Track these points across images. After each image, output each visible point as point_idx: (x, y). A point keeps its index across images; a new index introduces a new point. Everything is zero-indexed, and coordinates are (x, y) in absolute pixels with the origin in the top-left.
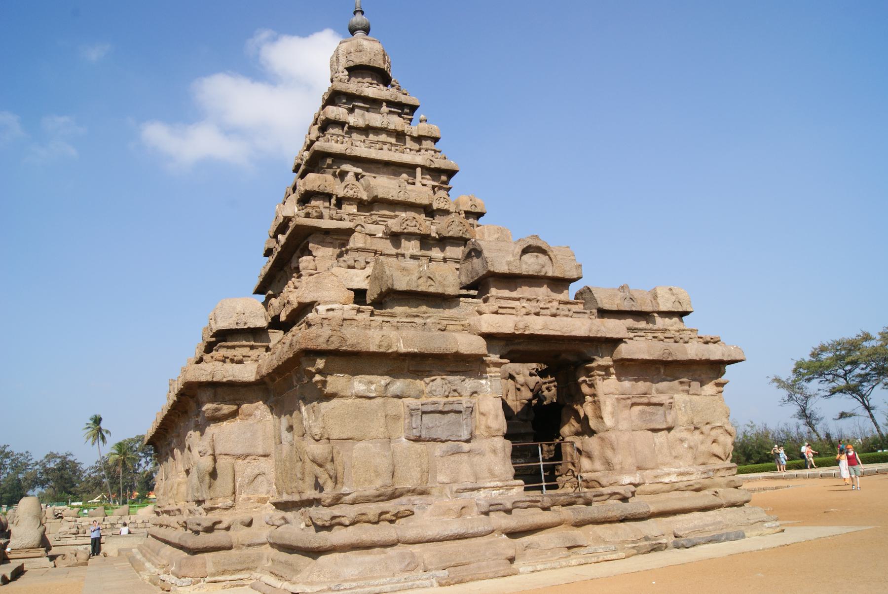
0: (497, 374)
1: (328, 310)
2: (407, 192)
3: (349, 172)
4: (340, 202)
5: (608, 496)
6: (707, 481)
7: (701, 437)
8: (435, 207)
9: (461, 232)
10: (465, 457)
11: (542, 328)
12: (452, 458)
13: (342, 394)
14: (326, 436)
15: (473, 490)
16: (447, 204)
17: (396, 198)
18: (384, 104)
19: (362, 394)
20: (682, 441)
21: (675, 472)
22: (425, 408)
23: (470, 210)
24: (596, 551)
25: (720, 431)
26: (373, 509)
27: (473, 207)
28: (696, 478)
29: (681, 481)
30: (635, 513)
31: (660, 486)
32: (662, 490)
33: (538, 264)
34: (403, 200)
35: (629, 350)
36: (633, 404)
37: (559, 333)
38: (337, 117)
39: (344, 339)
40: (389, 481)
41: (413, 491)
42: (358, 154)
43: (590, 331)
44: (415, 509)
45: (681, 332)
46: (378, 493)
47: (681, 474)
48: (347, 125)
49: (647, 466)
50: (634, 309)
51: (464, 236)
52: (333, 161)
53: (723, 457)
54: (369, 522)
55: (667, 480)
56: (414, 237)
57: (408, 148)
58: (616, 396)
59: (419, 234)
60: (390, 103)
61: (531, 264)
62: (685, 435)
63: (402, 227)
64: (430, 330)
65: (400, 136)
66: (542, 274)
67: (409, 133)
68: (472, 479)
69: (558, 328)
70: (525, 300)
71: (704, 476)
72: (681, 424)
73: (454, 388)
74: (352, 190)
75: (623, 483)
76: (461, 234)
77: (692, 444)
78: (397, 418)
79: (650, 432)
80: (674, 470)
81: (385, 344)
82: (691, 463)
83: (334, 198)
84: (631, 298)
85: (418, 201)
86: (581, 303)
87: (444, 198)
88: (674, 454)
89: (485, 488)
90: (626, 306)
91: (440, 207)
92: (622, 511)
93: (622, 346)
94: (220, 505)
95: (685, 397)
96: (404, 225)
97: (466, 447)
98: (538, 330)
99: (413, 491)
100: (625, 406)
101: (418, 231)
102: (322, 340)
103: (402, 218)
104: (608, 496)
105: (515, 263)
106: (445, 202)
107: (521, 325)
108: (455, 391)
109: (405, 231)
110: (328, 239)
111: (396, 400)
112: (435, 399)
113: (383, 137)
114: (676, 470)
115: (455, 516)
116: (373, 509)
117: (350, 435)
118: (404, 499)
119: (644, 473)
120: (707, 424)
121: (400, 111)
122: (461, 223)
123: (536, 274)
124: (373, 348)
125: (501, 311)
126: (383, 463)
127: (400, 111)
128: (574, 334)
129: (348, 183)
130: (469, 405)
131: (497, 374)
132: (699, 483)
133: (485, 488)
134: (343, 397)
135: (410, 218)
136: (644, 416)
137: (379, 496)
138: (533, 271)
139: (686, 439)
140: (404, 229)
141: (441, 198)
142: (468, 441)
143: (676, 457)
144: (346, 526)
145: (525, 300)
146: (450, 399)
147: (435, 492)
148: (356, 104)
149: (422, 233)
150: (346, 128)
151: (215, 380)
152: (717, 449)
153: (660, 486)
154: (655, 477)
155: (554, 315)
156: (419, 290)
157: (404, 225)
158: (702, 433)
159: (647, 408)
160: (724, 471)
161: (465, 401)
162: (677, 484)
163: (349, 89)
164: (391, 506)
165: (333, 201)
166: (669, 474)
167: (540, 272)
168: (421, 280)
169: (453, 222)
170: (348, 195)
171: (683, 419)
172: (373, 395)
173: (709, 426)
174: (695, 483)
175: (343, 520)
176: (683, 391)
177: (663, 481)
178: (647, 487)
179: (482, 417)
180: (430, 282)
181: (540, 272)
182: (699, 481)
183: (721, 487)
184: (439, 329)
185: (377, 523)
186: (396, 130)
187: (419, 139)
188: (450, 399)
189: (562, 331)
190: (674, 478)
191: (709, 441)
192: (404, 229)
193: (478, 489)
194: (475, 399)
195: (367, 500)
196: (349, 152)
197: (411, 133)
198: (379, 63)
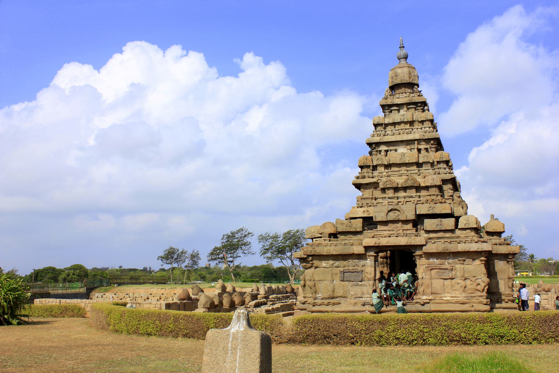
0: (372, 259)
1: (316, 240)
4: (375, 168)
5: (415, 303)
6: (468, 300)
7: (471, 282)
8: (421, 161)
9: (412, 184)
10: (360, 287)
12: (355, 287)
13: (319, 267)
14: (313, 279)
15: (360, 297)
17: (399, 162)
18: (405, 106)
19: (325, 267)
20: (458, 284)
21: (449, 296)
22: (345, 271)
23: (439, 160)
25: (480, 280)
26: (326, 301)
27: (441, 158)
28: (461, 298)
29: (453, 300)
33: (395, 216)
35: (431, 248)
36: (432, 269)
37: (394, 245)
39: (315, 251)
40: (332, 294)
41: (341, 297)
43: (407, 243)
44: (341, 302)
45: (467, 237)
46: (328, 297)
48: (384, 125)
50: (442, 229)
51: (413, 185)
52: (375, 146)
53: (481, 291)
54: (325, 305)
55: (445, 299)
56: (391, 189)
58: (426, 265)
59: (393, 187)
60: (408, 104)
61: (392, 216)
62: (460, 281)
63: (384, 186)
64: (347, 245)
66: (397, 219)
67: (417, 120)
68: (361, 294)
69: (393, 243)
70: (388, 231)
71: (466, 298)
72: (458, 277)
73: (356, 264)
76: (412, 185)
77: (462, 285)
78: (336, 274)
79: (442, 280)
80: (449, 295)
81: (328, 252)
82: (461, 293)
83: (371, 167)
85: (410, 161)
86: (414, 229)
89: (364, 297)
90: (438, 228)
92: (417, 309)
93: (424, 247)
94: (307, 296)
95: (462, 266)
96: (385, 184)
97: (360, 283)
98: (385, 244)
99: (341, 297)
100: (428, 270)
101: (391, 186)
102: (309, 252)
104: (415, 303)
105: (384, 217)
107: (377, 243)
108: (357, 265)
109: (386, 187)
110: (368, 187)
111: (336, 268)
112: (349, 268)
113: (403, 126)
114: (450, 295)
115: (353, 305)
116: (326, 301)
117: (321, 279)
118: (337, 299)
120: (474, 277)
121: (415, 106)
124: (325, 254)
125: (375, 236)
126: (330, 288)
127: (415, 106)
128: (400, 244)
130: (361, 270)
131: (372, 259)
132: (462, 301)
133: (364, 297)
134: (319, 267)
135: (388, 181)
136: (438, 273)
137: (329, 298)
139: (460, 283)
140: (385, 186)
142: (361, 281)
143: (455, 290)
144: (319, 306)
145: (388, 231)
146: (355, 268)
147: (349, 297)
149: (393, 186)
150: (383, 126)
151: (301, 257)
152: (479, 287)
153: (442, 301)
154: (441, 297)
155: (397, 237)
156: (346, 231)
157: (385, 184)
158: (471, 281)
159: (440, 271)
160: (478, 297)
161: (359, 269)
162: (451, 301)
164: (332, 301)
165: (371, 168)
166: (446, 297)
167: (396, 219)
168: (347, 227)
169: (408, 179)
171: (459, 274)
172: (328, 267)
173: (475, 278)
174: (460, 301)
175: (317, 304)
176: (460, 263)
179: (366, 274)
180: (350, 228)
181: (396, 219)
183: (475, 303)
184: (350, 245)
185: (328, 305)
186: (408, 121)
188: (355, 268)
190: (448, 298)
191: (475, 284)
192: (385, 186)
193: (362, 297)
194: (363, 268)
195: (326, 299)
196: (382, 140)
197: (418, 119)
198: (406, 80)
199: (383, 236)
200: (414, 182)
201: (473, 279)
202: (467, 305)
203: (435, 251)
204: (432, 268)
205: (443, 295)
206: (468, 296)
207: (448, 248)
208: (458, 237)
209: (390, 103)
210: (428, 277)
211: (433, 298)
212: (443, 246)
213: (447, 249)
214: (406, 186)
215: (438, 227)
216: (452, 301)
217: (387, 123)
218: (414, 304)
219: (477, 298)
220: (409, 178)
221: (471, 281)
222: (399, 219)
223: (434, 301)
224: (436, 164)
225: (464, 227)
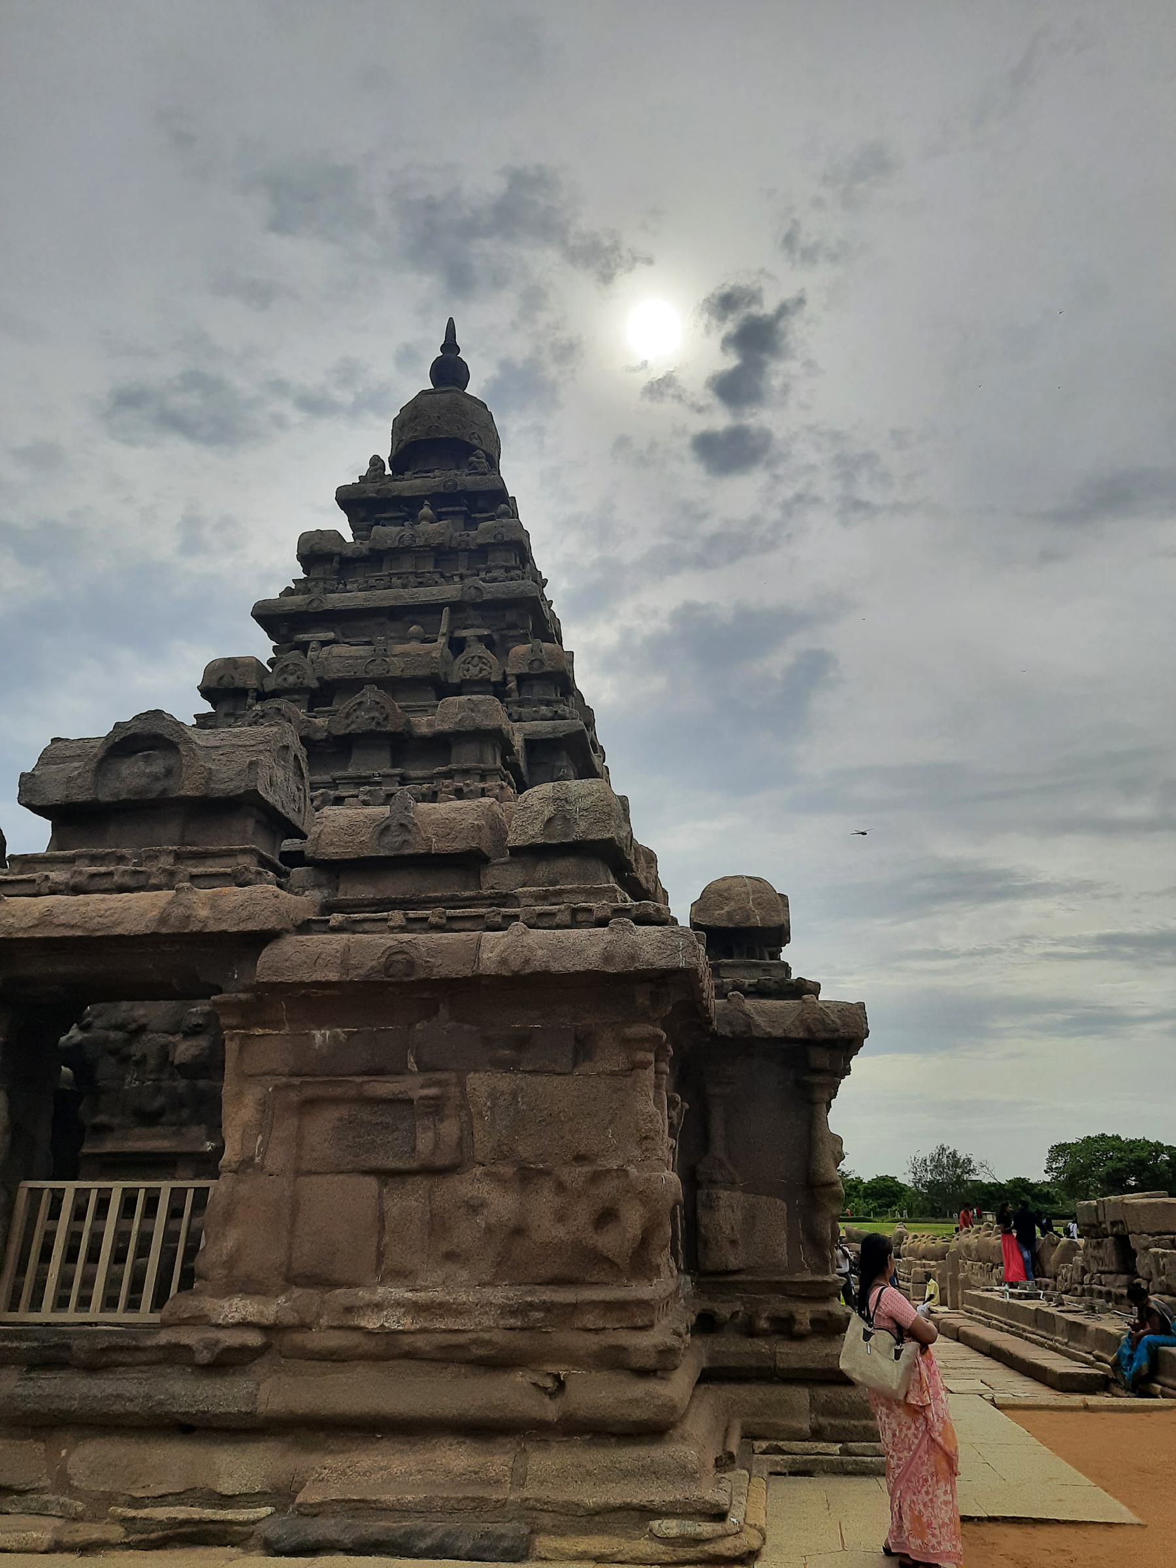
2: (388, 659)
3: (310, 642)
6: (522, 1341)
9: (374, 723)
11: (36, 922)
16: (485, 667)
20: (474, 1208)
23: (526, 670)
24: (46, 1508)
27: (536, 664)
30: (204, 1412)
31: (352, 1339)
32: (360, 1350)
34: (376, 676)
36: (310, 1104)
37: (79, 933)
38: (316, 547)
42: (330, 607)
47: (418, 1309)
48: (337, 558)
49: (336, 1276)
55: (371, 1322)
57: (456, 575)
65: (442, 555)
67: (463, 546)
72: (480, 1159)
74: (292, 674)
75: (220, 1321)
76: (373, 726)
84: (402, 825)
87: (479, 657)
88: (444, 1247)
91: (468, 677)
103: (254, 714)
106: (480, 665)
114: (409, 1294)
119: (327, 1296)
120: (580, 1159)
122: (378, 703)
123: (137, 797)
128: (119, 930)
129: (285, 664)
132: (488, 1343)
138: (129, 792)
139: (483, 1204)
141: (473, 657)
148: (383, 515)
152: (609, 1241)
154: (349, 1310)
163: (365, 492)
166: (378, 1307)
170: (286, 685)
173: (586, 1169)
174: (474, 1342)
177: (363, 1324)
178: (318, 1340)
182: (486, 1336)
187: (482, 552)
189: (87, 925)
191: (583, 1214)
196: (315, 605)
199: (45, 887)
200: (381, 718)
201: (573, 1175)
202: (521, 1378)
203: (333, 976)
204: (309, 1092)
205: (363, 1294)
206: (531, 1306)
207: (414, 953)
208: (505, 899)
209: (375, 495)
210: (277, 1159)
211: (290, 1318)
212: (388, 940)
213: (411, 964)
214: (347, 731)
215: (387, 839)
216: (421, 1342)
217: (350, 554)
218: (153, 1363)
219: (590, 1320)
220: (363, 699)
221: (561, 1187)
222: (165, 790)
223: (299, 1338)
224: (512, 685)
225: (540, 840)
